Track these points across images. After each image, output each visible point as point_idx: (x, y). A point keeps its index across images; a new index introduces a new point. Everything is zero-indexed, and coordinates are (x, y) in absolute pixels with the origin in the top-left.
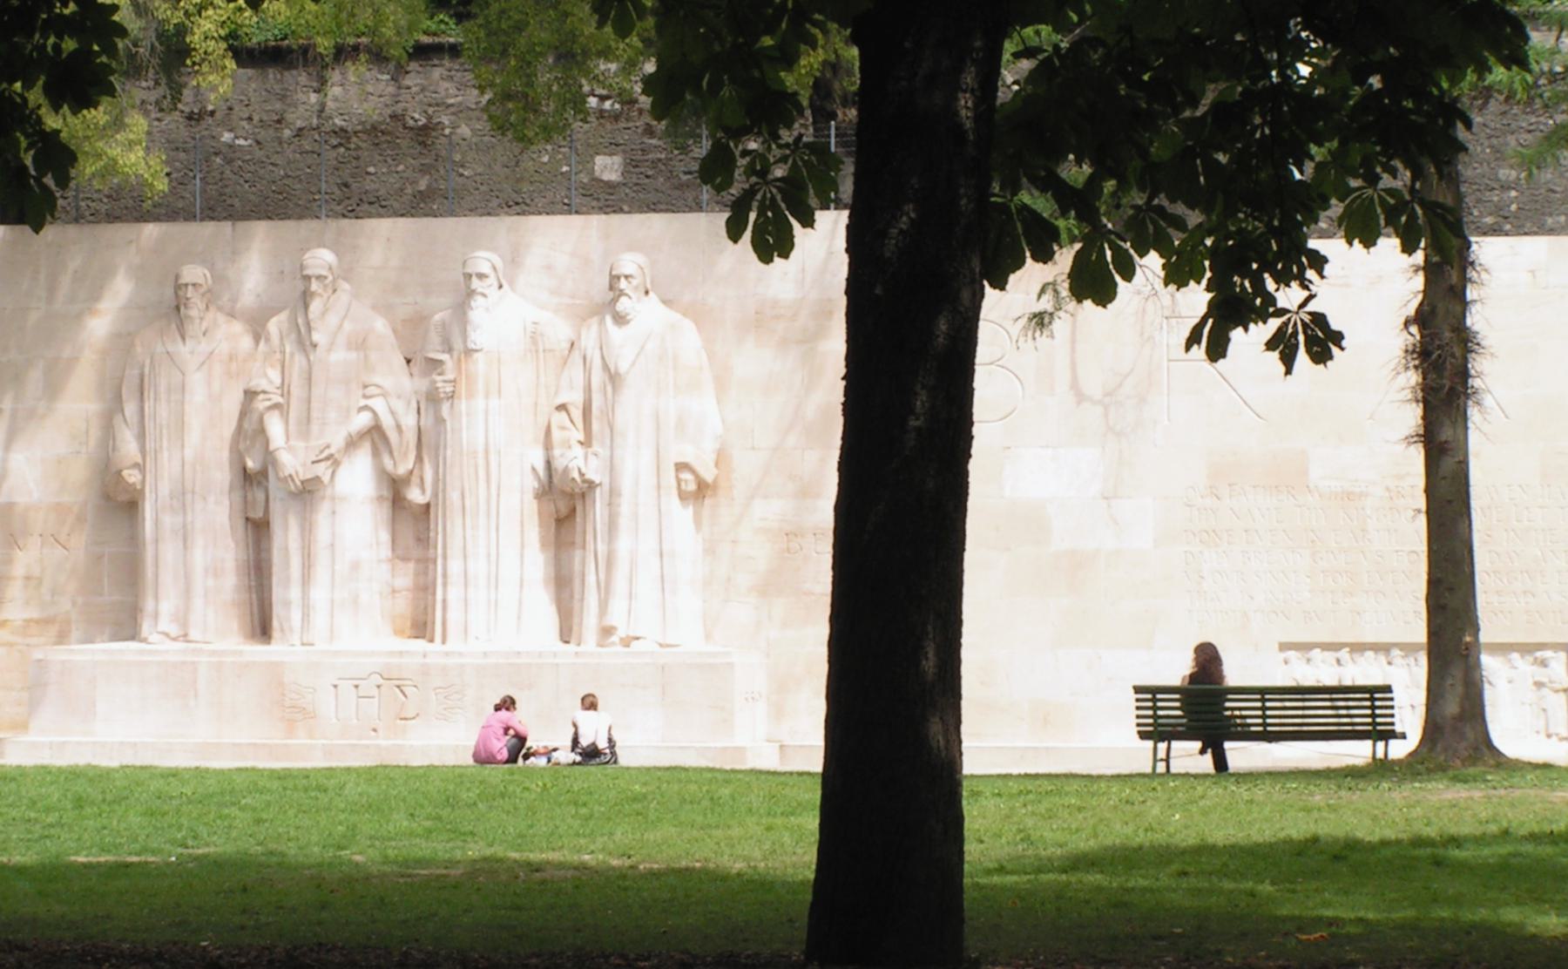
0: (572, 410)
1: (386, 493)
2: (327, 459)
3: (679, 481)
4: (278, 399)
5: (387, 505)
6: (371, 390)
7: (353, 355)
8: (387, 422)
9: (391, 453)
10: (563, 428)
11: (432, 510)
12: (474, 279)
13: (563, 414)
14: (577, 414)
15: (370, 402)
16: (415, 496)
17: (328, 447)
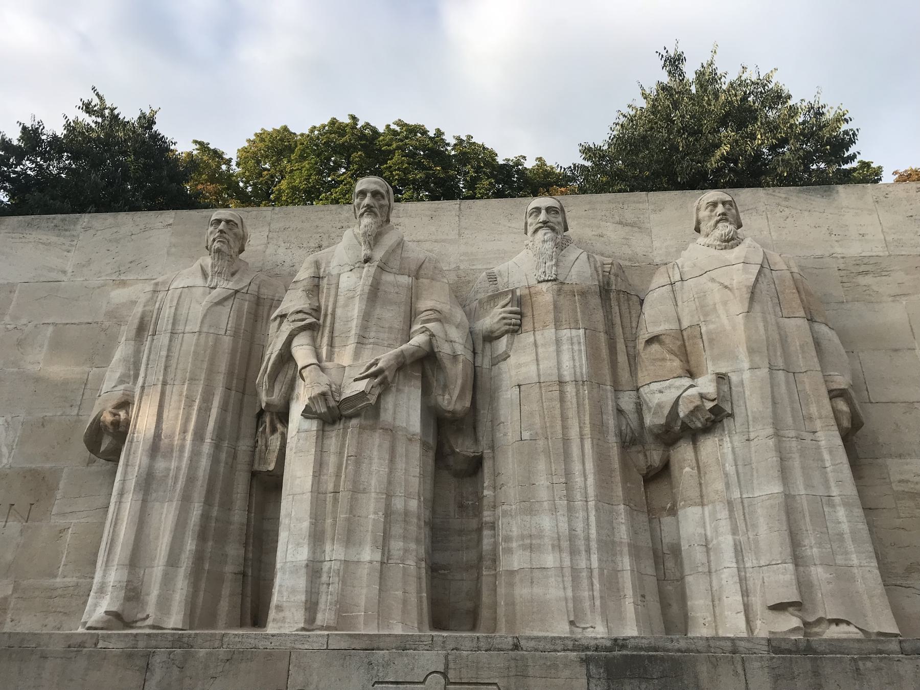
0: (667, 340)
1: (431, 441)
2: (374, 375)
3: (835, 411)
4: (311, 320)
5: (431, 454)
6: (423, 316)
7: (405, 280)
8: (444, 349)
9: (445, 387)
10: (664, 359)
11: (487, 465)
12: (543, 212)
13: (655, 347)
14: (675, 345)
15: (428, 325)
16: (464, 447)
17: (375, 364)
